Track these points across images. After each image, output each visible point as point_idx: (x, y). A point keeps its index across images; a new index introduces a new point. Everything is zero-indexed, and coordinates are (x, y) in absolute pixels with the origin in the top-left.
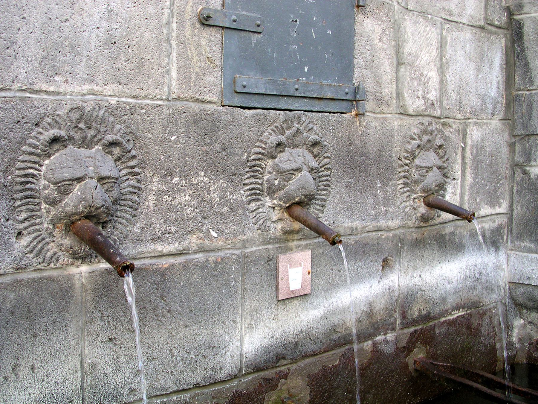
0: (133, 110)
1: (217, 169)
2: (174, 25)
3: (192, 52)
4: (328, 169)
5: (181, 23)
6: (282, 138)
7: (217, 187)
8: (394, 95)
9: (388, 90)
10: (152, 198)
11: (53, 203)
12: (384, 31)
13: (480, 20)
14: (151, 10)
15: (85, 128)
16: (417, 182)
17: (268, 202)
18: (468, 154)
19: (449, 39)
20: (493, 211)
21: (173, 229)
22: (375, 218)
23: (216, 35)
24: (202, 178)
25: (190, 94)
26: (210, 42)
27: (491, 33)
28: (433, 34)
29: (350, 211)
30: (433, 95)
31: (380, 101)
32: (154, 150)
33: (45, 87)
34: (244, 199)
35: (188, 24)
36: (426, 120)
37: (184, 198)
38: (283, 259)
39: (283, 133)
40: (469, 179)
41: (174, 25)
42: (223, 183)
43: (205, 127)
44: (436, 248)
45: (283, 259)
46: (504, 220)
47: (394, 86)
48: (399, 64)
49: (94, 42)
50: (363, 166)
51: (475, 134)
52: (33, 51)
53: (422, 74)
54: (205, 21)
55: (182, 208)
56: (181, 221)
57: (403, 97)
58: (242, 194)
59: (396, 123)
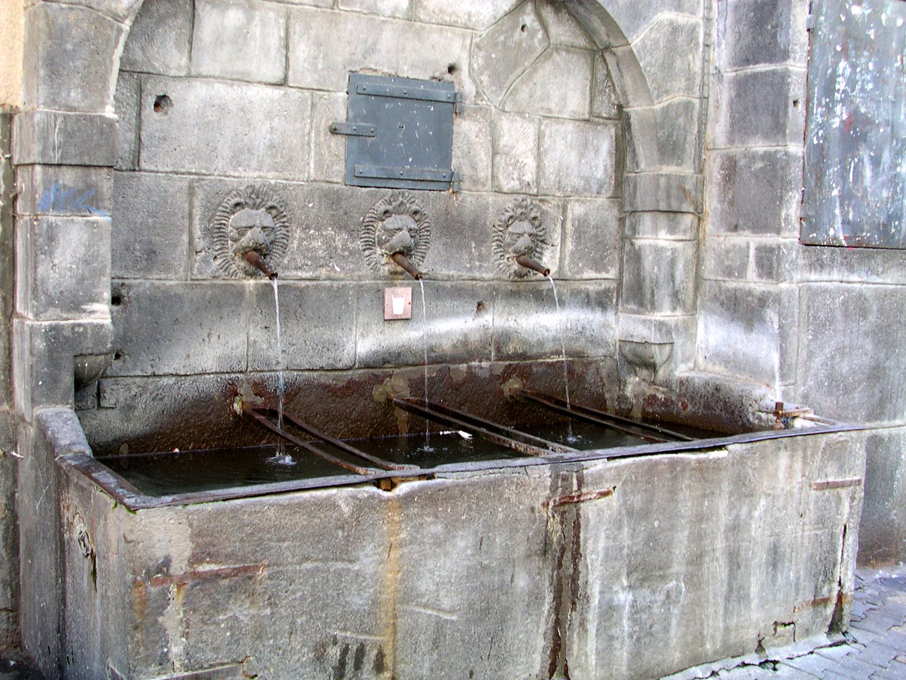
0: (285, 187)
1: (341, 226)
2: (313, 135)
3: (325, 151)
4: (428, 231)
5: (318, 134)
6: (389, 207)
7: (339, 240)
8: (490, 178)
9: (484, 173)
10: (296, 243)
11: (235, 240)
12: (480, 130)
13: (583, 114)
14: (298, 125)
15: (255, 197)
16: (509, 245)
17: (379, 251)
18: (569, 225)
19: (547, 132)
20: (599, 276)
21: (309, 263)
22: (470, 270)
24: (330, 231)
25: (323, 177)
26: (338, 145)
27: (598, 124)
29: (447, 263)
30: (529, 177)
31: (475, 181)
32: (298, 212)
33: (233, 173)
34: (361, 248)
35: (322, 134)
36: (520, 198)
37: (317, 244)
38: (388, 292)
39: (390, 204)
40: (570, 246)
41: (313, 135)
43: (332, 199)
44: (532, 300)
45: (388, 292)
46: (613, 285)
47: (490, 171)
48: (495, 153)
49: (262, 147)
50: (460, 230)
51: (576, 209)
52: (227, 153)
53: (518, 161)
54: (334, 131)
55: (316, 250)
56: (314, 259)
57: (498, 178)
58: (359, 244)
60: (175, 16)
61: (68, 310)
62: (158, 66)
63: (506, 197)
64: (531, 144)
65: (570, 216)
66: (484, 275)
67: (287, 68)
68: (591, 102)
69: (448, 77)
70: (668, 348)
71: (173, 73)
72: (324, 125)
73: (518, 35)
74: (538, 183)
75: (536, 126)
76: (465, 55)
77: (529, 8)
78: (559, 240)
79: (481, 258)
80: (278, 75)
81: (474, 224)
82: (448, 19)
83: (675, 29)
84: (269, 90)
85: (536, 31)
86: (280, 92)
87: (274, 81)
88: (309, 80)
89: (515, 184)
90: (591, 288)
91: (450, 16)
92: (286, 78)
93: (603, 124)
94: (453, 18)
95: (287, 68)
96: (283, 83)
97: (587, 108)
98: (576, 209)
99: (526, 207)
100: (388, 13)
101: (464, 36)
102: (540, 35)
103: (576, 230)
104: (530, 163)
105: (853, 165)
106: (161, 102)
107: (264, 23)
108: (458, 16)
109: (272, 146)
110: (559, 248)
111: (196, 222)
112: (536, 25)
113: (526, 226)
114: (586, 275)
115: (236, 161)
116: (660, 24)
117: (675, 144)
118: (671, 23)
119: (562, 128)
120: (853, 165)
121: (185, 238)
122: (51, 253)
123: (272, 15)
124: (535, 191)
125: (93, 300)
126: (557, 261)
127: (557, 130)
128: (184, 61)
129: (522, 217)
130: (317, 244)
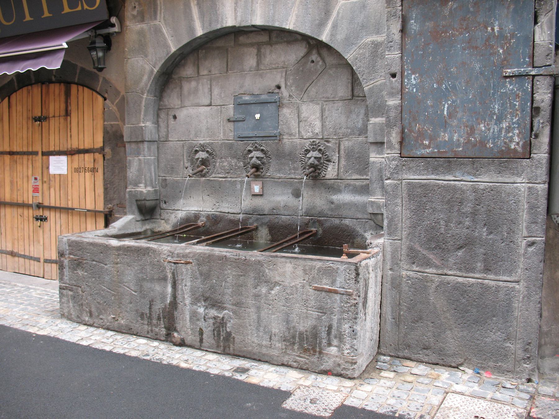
0: (212, 143)
1: (234, 157)
3: (226, 128)
5: (223, 122)
7: (234, 162)
8: (297, 132)
9: (295, 130)
14: (216, 120)
15: (203, 148)
18: (342, 152)
20: (362, 178)
22: (289, 174)
23: (232, 124)
24: (229, 159)
26: (231, 125)
27: (358, 100)
28: (317, 108)
29: (279, 171)
30: (317, 130)
31: (291, 135)
32: (218, 152)
36: (312, 140)
37: (225, 164)
40: (343, 162)
42: (235, 160)
43: (230, 147)
48: (299, 122)
51: (346, 144)
52: (193, 133)
54: (229, 120)
55: (224, 166)
59: (298, 141)
60: (176, 88)
61: (135, 186)
62: (172, 106)
63: (306, 141)
64: (318, 114)
65: (342, 147)
66: (297, 177)
67: (211, 99)
68: (353, 90)
69: (277, 91)
70: (380, 216)
71: (177, 107)
72: (226, 118)
73: (310, 65)
74: (322, 131)
75: (320, 106)
76: (283, 80)
77: (314, 52)
78: (337, 160)
79: (295, 169)
80: (207, 102)
81: (290, 154)
82: (274, 66)
83: (376, 45)
84: (206, 108)
85: (318, 62)
86: (210, 108)
87: (207, 104)
88: (219, 102)
89: (310, 135)
90: (358, 183)
91: (275, 64)
92: (211, 102)
93: (361, 99)
94: (277, 65)
95: (211, 99)
96: (210, 105)
97: (350, 93)
98: (346, 144)
99: (316, 145)
100: (248, 70)
101: (282, 72)
102: (320, 63)
103: (346, 156)
104: (318, 124)
105: (446, 106)
106: (175, 117)
107: (203, 85)
108: (278, 64)
109: (207, 128)
110: (337, 164)
111: (185, 157)
112: (319, 59)
113: (316, 154)
114: (353, 177)
115: (196, 136)
116: (366, 45)
117: (379, 106)
118: (373, 42)
119: (336, 105)
120: (446, 106)
121: (182, 163)
122: (130, 169)
123: (205, 80)
124: (321, 137)
125: (140, 183)
126: (336, 170)
127: (332, 107)
128: (179, 103)
129: (314, 150)
130: (225, 164)
